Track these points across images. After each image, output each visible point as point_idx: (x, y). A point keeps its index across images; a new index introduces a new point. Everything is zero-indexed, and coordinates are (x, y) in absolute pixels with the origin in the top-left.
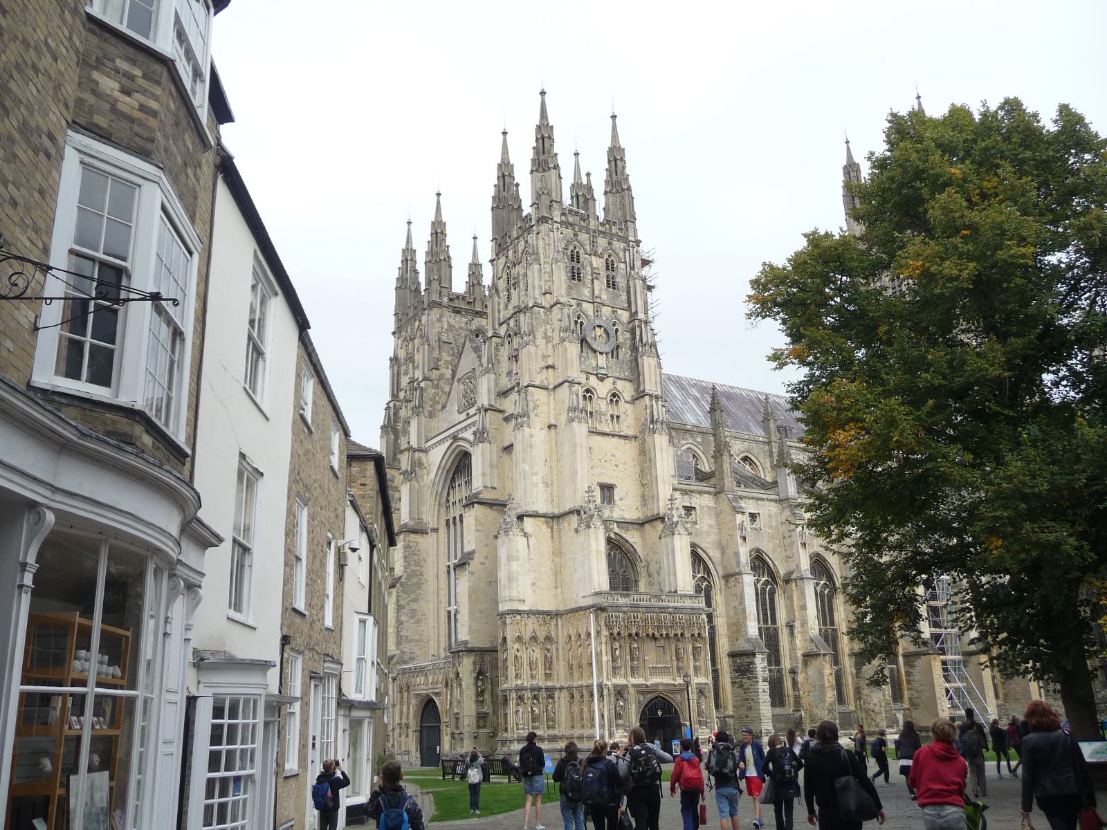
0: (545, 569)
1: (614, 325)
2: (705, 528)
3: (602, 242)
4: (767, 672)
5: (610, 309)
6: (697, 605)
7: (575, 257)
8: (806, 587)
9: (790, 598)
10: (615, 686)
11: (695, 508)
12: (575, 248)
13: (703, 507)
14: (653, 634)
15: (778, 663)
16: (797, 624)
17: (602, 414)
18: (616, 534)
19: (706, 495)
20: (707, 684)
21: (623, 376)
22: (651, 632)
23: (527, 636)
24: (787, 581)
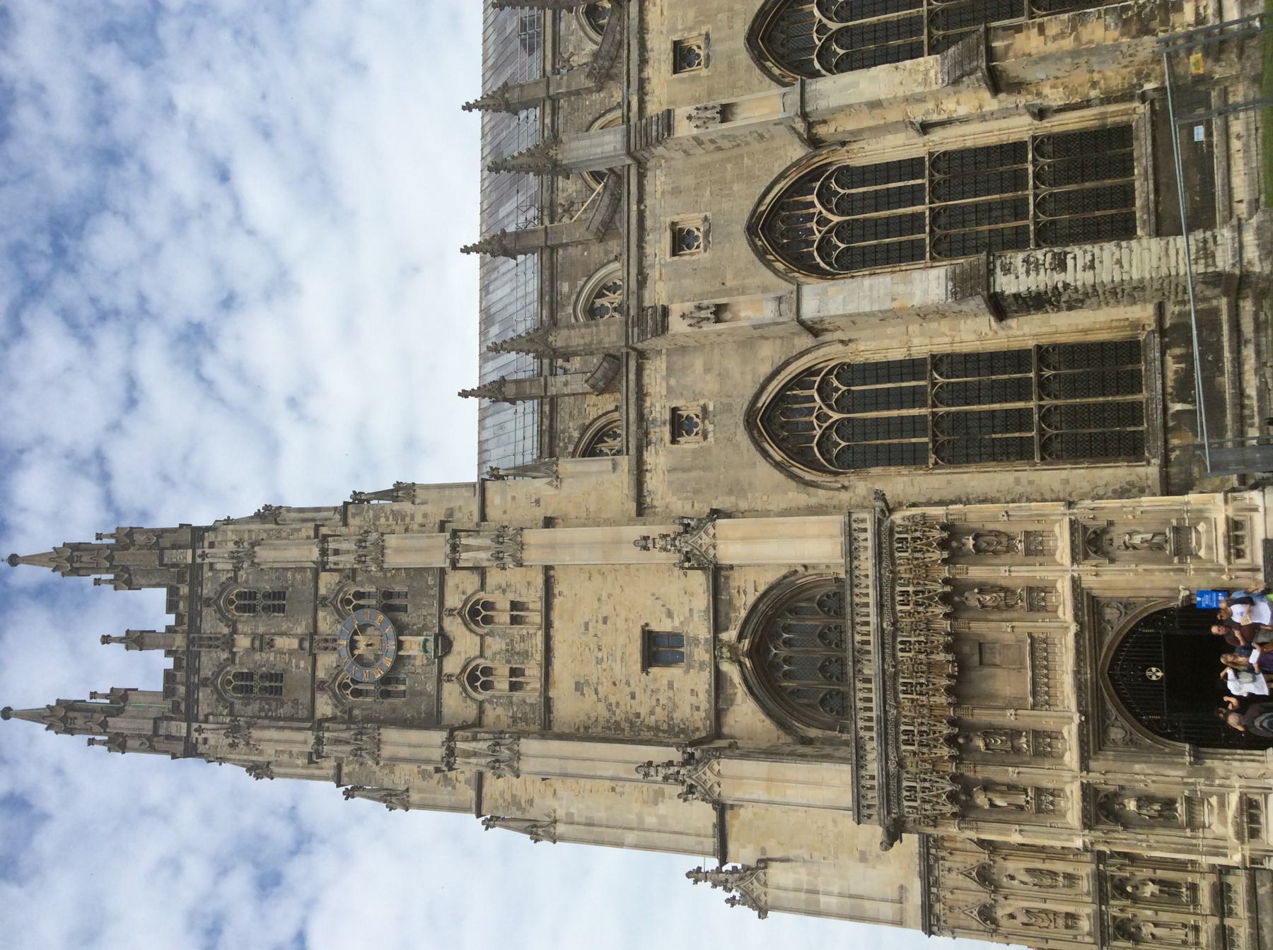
0: (830, 825)
1: (349, 602)
2: (710, 385)
3: (211, 624)
4: (1039, 254)
5: (321, 614)
6: (869, 535)
7: (245, 683)
8: (823, 104)
9: (857, 135)
10: (1089, 822)
11: (674, 411)
12: (229, 682)
13: (670, 389)
14: (949, 691)
15: (1015, 150)
16: (918, 113)
17: (511, 652)
18: (740, 637)
19: (646, 380)
20: (1072, 523)
21: (435, 591)
22: (942, 699)
23: (975, 895)
24: (814, 142)
